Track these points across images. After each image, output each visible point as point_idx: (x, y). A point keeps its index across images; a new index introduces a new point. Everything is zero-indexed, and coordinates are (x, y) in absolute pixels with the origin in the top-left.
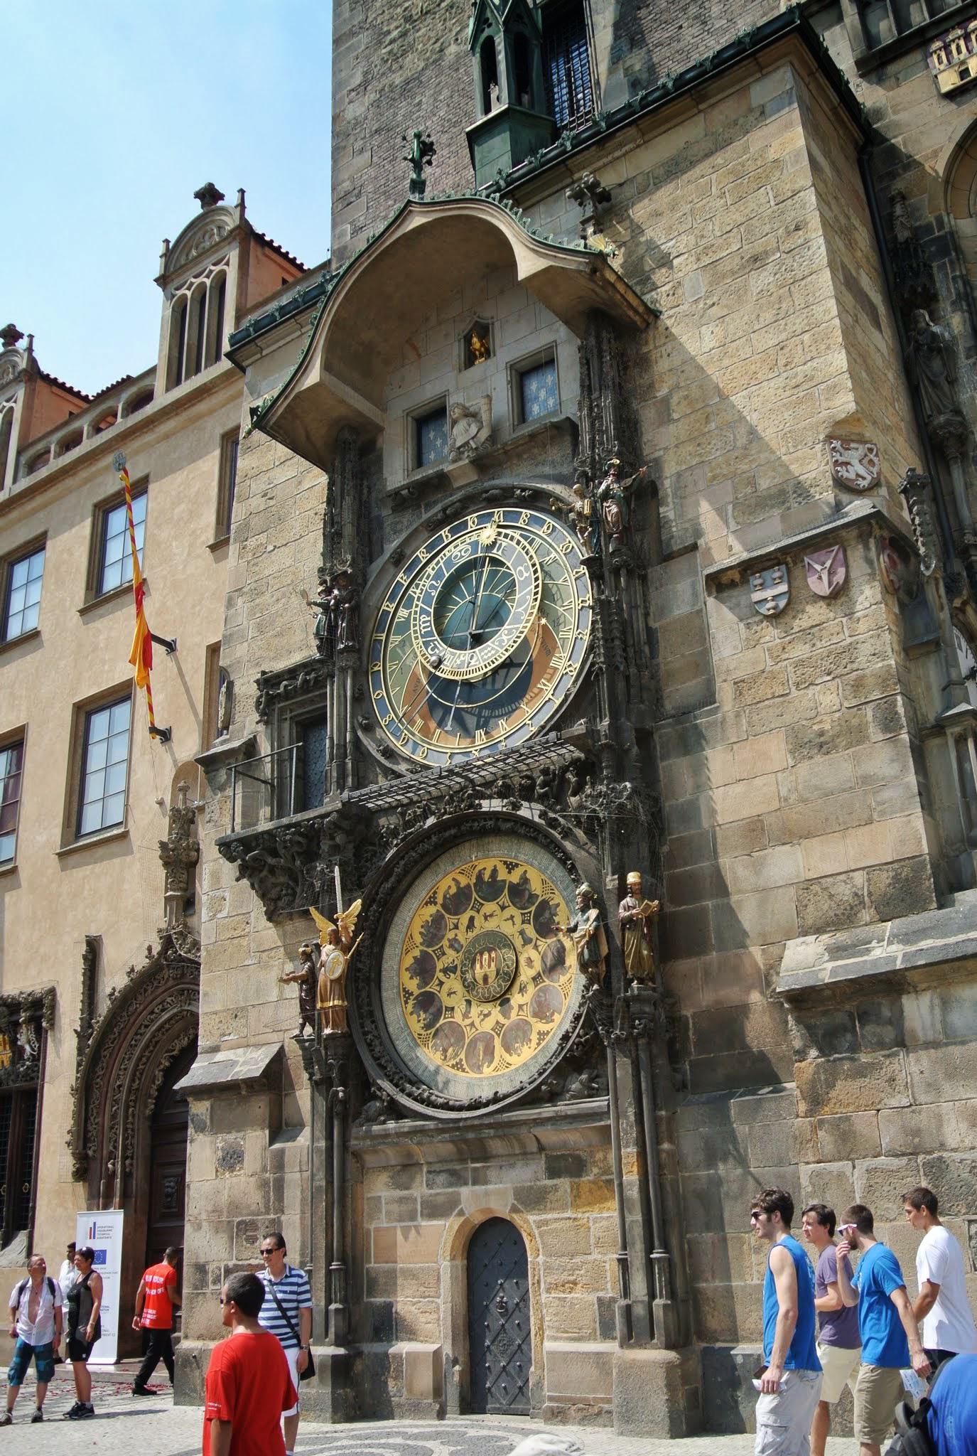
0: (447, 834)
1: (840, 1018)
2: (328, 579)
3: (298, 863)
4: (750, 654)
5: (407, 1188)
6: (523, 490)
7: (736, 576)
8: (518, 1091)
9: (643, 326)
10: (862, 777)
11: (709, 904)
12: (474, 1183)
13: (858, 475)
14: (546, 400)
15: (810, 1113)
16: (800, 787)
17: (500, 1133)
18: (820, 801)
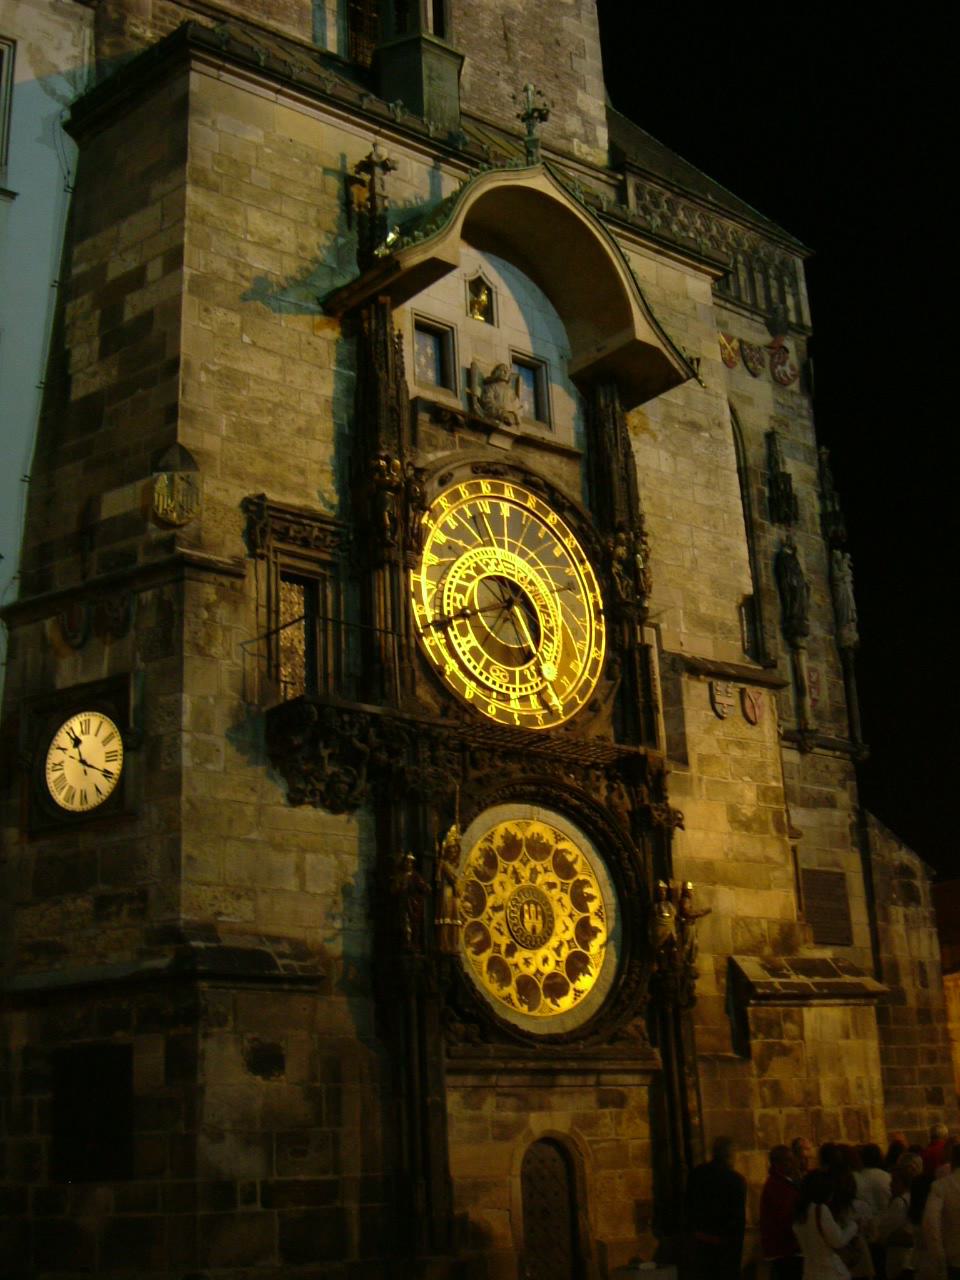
4: (706, 737)
5: (479, 1108)
6: (564, 497)
12: (542, 1107)
16: (735, 850)
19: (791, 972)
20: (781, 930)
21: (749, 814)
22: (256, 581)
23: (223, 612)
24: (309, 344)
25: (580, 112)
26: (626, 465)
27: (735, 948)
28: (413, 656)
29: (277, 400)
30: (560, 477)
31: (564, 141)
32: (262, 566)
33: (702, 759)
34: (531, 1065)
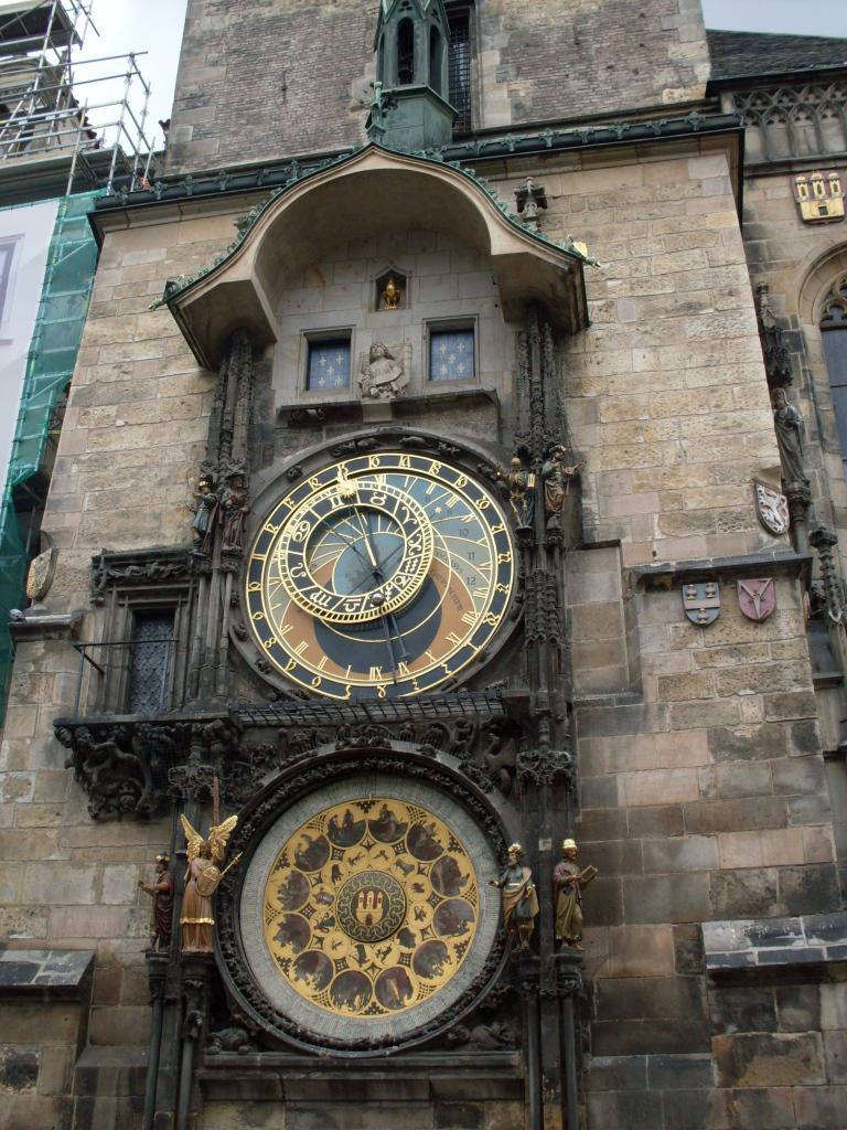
0: (345, 766)
1: (759, 999)
2: (215, 476)
3: (154, 763)
4: (676, 654)
6: (449, 445)
7: (668, 581)
8: (414, 1037)
9: (574, 328)
10: (778, 786)
11: (622, 878)
13: (775, 520)
14: (456, 365)
15: (725, 1084)
16: (719, 785)
17: (392, 1076)
18: (738, 800)
19: (804, 935)
20: (807, 880)
21: (749, 736)
22: (94, 631)
23: (49, 664)
24: (183, 403)
25: (670, 63)
26: (542, 382)
27: (715, 911)
28: (224, 656)
29: (142, 464)
30: (466, 425)
31: (648, 99)
32: (101, 614)
33: (667, 683)
34: (316, 1076)
